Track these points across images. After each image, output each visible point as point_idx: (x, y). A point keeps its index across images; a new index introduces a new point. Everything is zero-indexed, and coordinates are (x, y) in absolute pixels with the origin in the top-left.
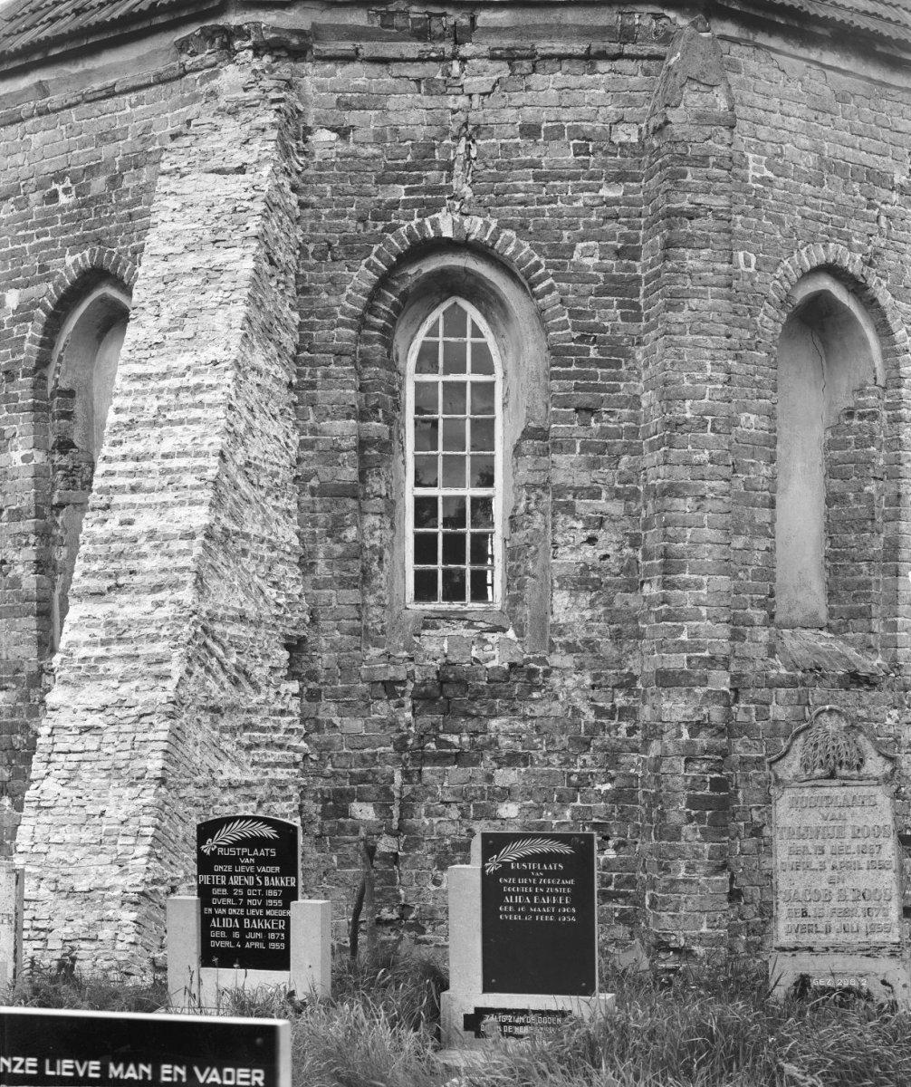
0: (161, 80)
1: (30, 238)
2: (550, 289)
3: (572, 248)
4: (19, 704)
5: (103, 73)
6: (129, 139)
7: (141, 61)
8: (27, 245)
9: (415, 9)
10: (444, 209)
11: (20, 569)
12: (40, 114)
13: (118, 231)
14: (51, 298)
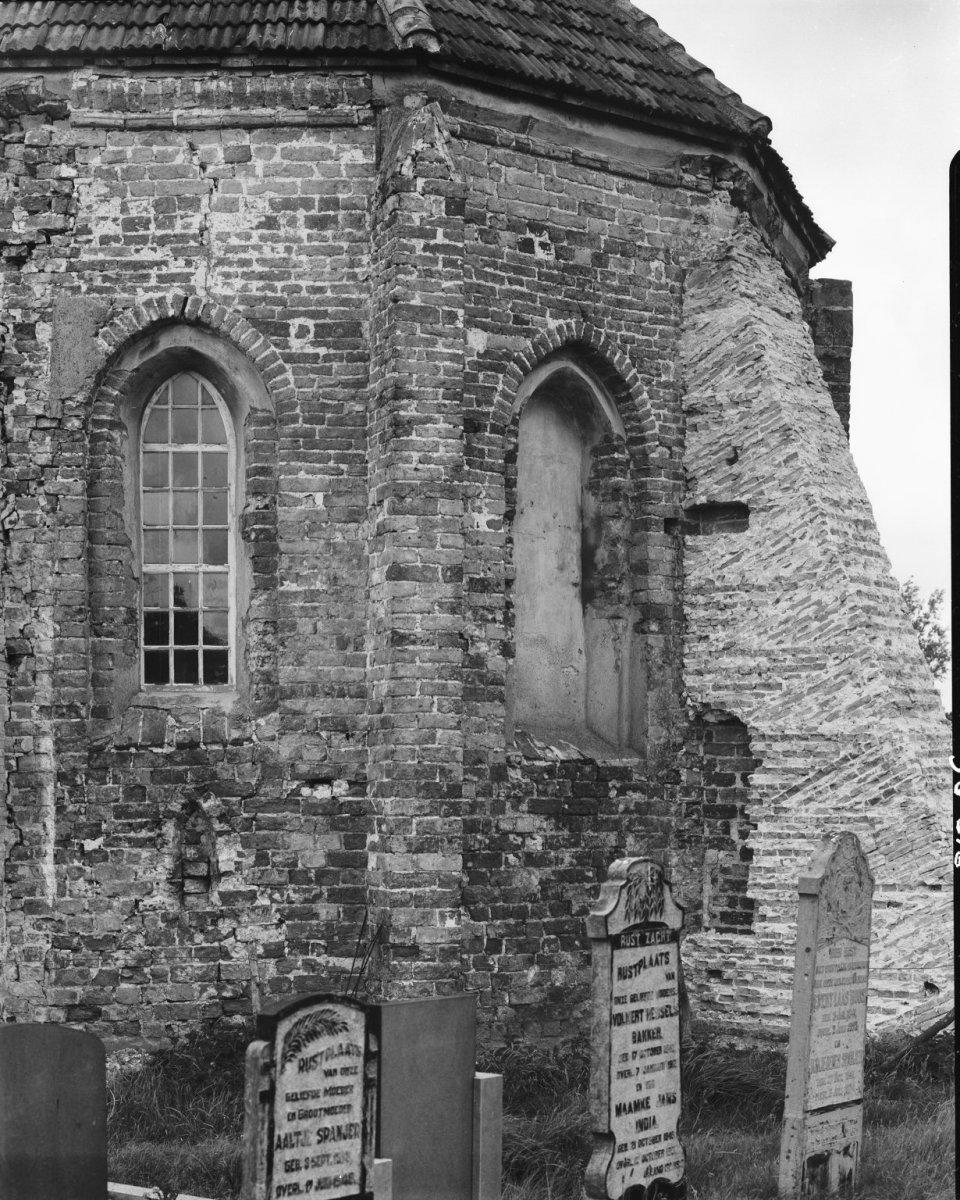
0: (655, 181)
1: (501, 280)
4: (480, 799)
5: (595, 143)
6: (616, 223)
7: (640, 153)
8: (497, 287)
11: (483, 648)
12: (516, 149)
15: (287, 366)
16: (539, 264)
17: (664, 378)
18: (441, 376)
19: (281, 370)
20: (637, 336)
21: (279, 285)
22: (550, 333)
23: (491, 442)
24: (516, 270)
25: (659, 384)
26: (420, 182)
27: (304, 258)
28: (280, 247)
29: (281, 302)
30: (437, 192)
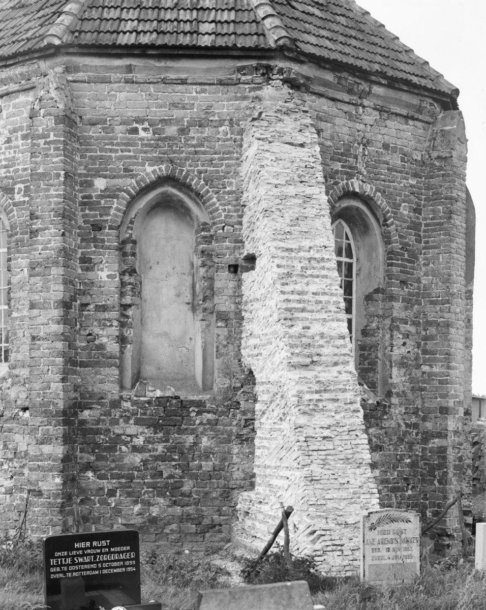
0: (221, 83)
1: (116, 151)
2: (392, 223)
3: (400, 205)
5: (178, 70)
6: (195, 110)
7: (208, 70)
8: (113, 155)
9: (350, 78)
10: (355, 178)
12: (127, 82)
13: (187, 159)
14: (134, 188)
15: (14, 208)
16: (142, 139)
17: (228, 189)
18: (53, 206)
19: (12, 211)
20: (209, 168)
21: (11, 169)
22: (147, 174)
23: (108, 235)
24: (125, 144)
25: (224, 192)
26: (42, 111)
27: (20, 155)
28: (12, 151)
29: (12, 178)
30: (50, 114)
